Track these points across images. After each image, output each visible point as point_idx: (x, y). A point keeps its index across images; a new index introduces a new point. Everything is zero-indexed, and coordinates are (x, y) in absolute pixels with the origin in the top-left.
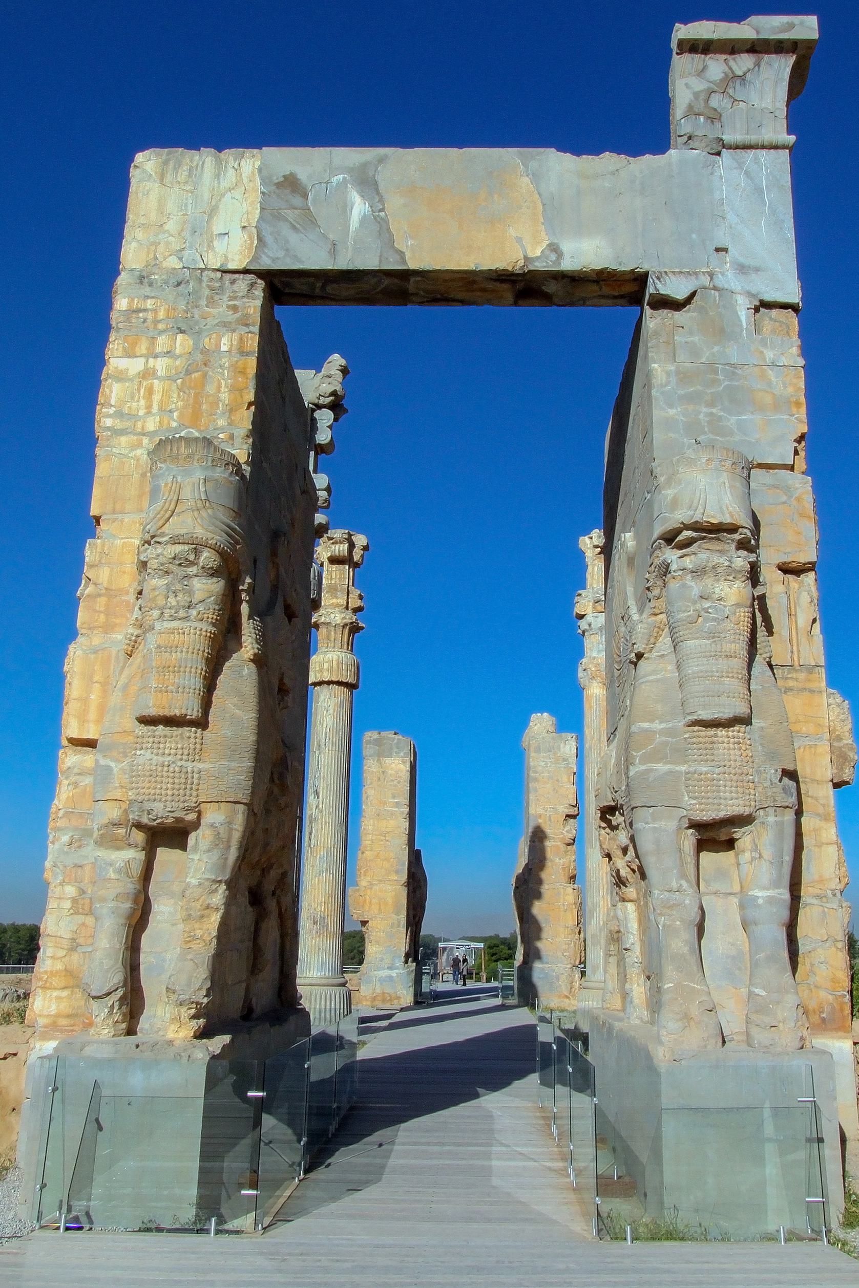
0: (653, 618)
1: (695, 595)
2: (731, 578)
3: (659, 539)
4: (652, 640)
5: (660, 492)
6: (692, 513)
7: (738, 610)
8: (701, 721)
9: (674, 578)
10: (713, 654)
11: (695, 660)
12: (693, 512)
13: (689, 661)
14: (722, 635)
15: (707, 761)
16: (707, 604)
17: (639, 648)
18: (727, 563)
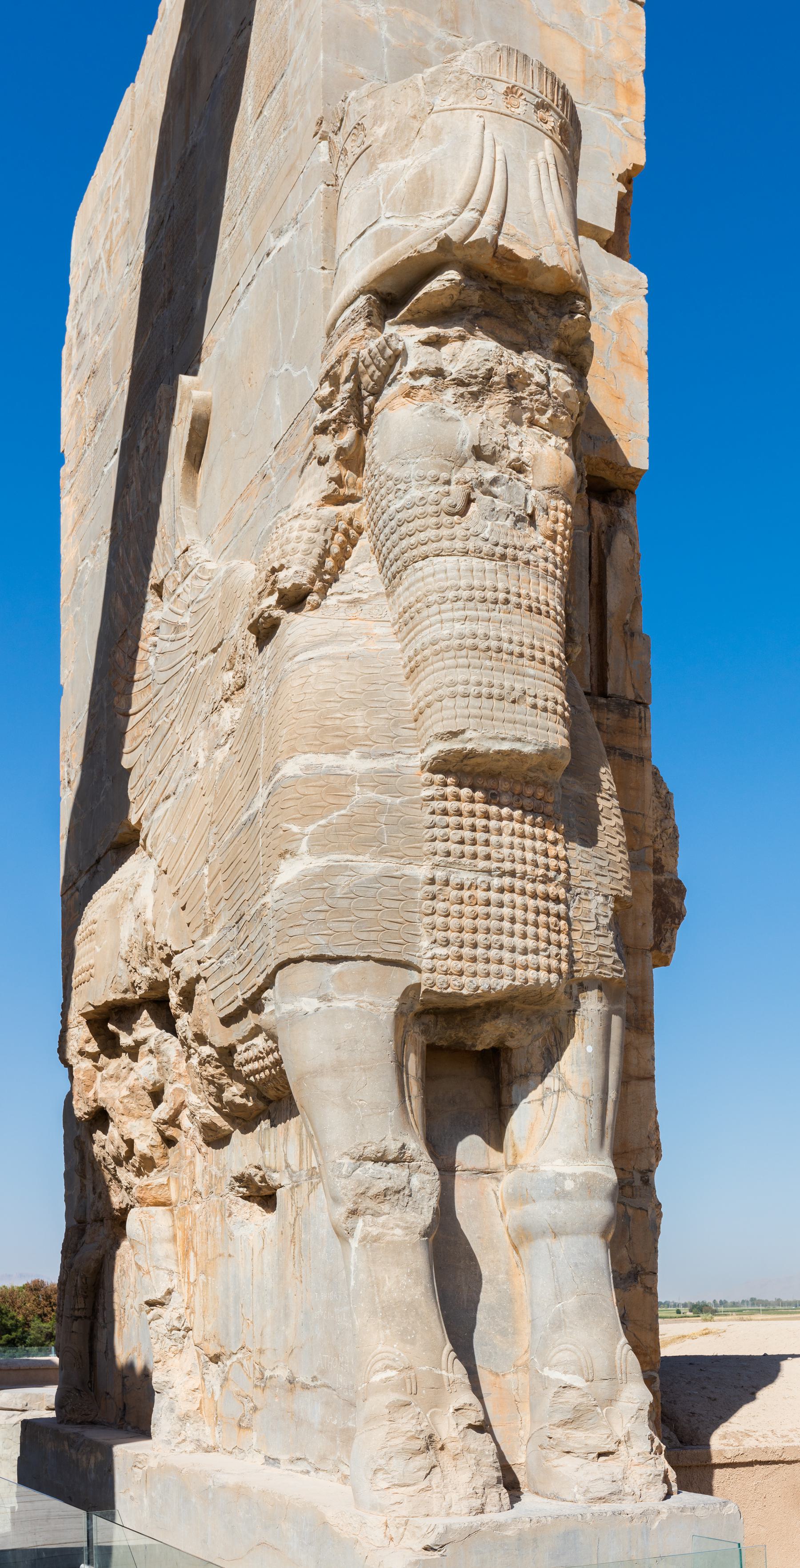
0: (331, 510)
1: (463, 441)
2: (544, 419)
3: (362, 292)
4: (329, 563)
5: (373, 166)
6: (469, 216)
7: (553, 503)
8: (471, 755)
9: (407, 395)
10: (501, 596)
11: (460, 604)
12: (476, 215)
13: (443, 607)
14: (520, 554)
15: (475, 856)
16: (489, 473)
17: (286, 580)
18: (539, 378)
